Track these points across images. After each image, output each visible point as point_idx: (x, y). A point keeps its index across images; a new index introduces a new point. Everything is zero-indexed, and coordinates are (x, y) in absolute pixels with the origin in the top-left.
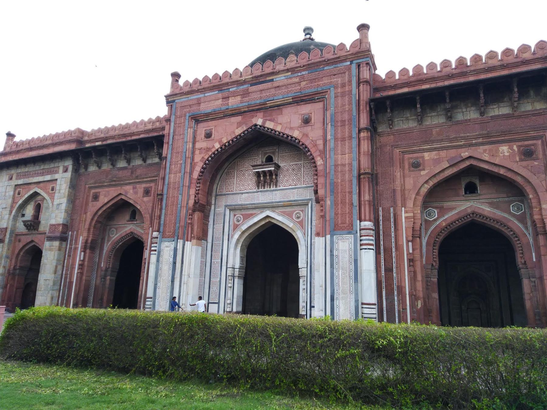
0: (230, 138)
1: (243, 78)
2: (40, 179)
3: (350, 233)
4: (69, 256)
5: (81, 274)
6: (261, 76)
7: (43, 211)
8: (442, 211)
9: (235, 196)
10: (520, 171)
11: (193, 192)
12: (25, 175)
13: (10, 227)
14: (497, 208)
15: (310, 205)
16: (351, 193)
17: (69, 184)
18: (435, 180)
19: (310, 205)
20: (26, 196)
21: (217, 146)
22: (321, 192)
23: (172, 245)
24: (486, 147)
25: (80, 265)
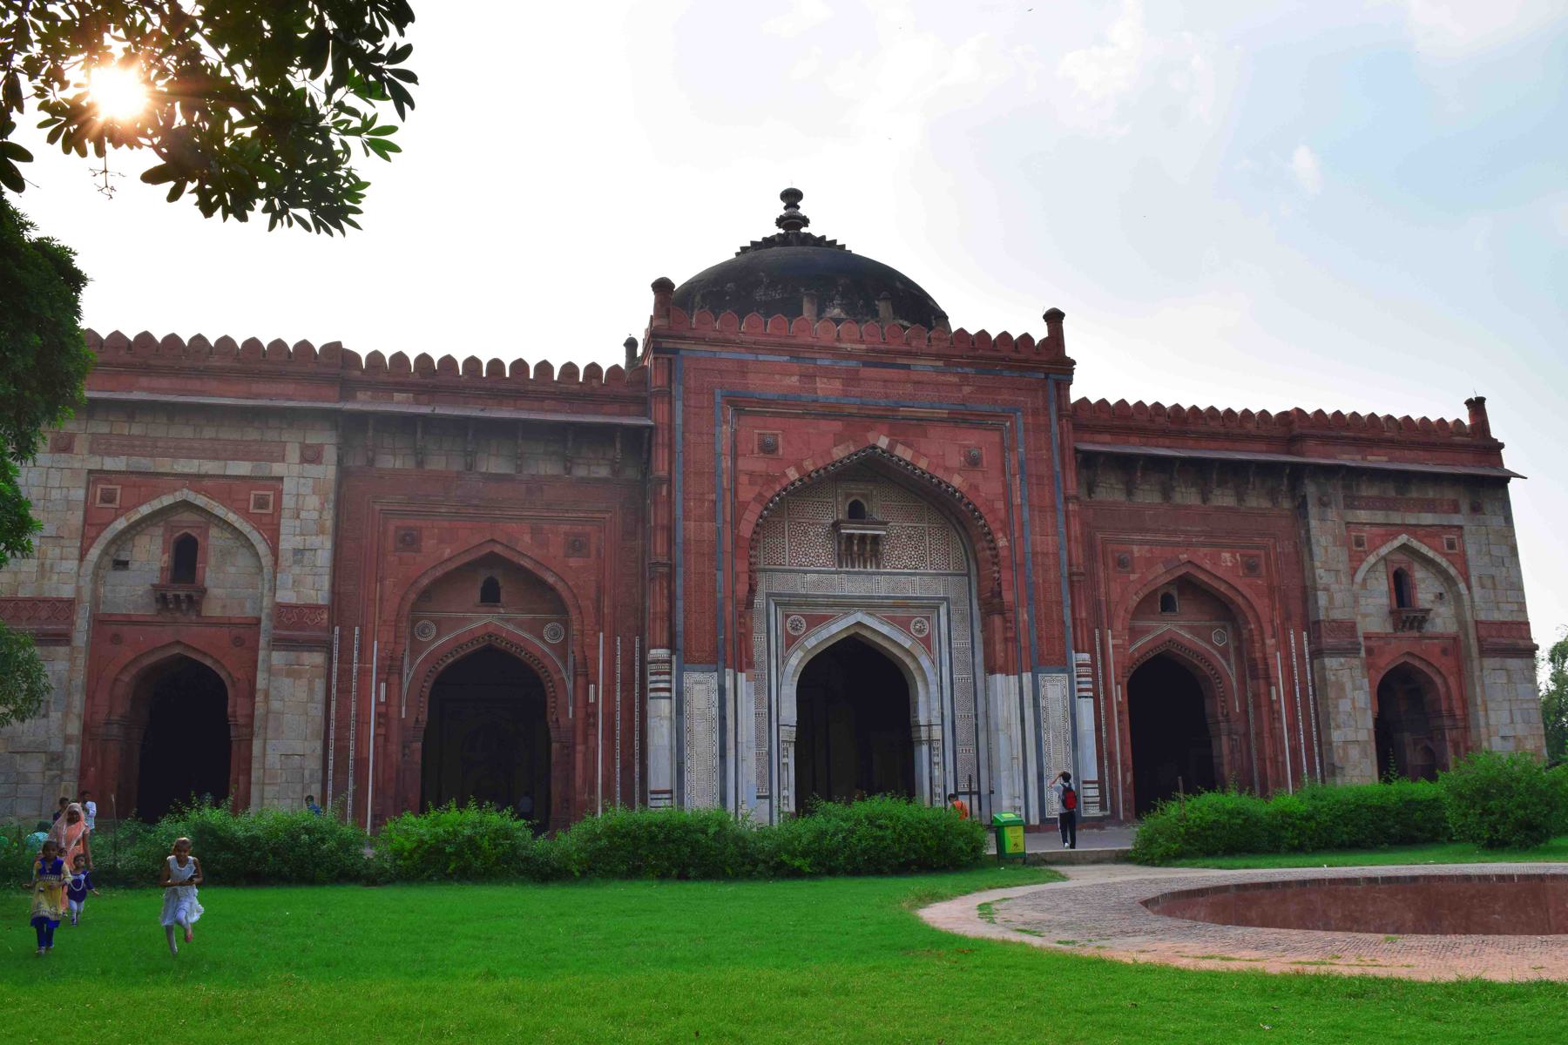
0: (820, 464)
1: (849, 346)
2: (210, 467)
3: (1063, 671)
4: (344, 691)
5: (384, 739)
6: (887, 352)
7: (212, 560)
8: (1134, 634)
9: (789, 576)
10: (1247, 592)
11: (742, 566)
12: (128, 447)
13: (86, 595)
14: (1198, 635)
15: (943, 610)
16: (1060, 603)
17: (332, 496)
18: (1146, 591)
19: (943, 610)
20: (145, 510)
21: (793, 474)
22: (1008, 596)
23: (712, 680)
24: (1206, 550)
25: (378, 715)
